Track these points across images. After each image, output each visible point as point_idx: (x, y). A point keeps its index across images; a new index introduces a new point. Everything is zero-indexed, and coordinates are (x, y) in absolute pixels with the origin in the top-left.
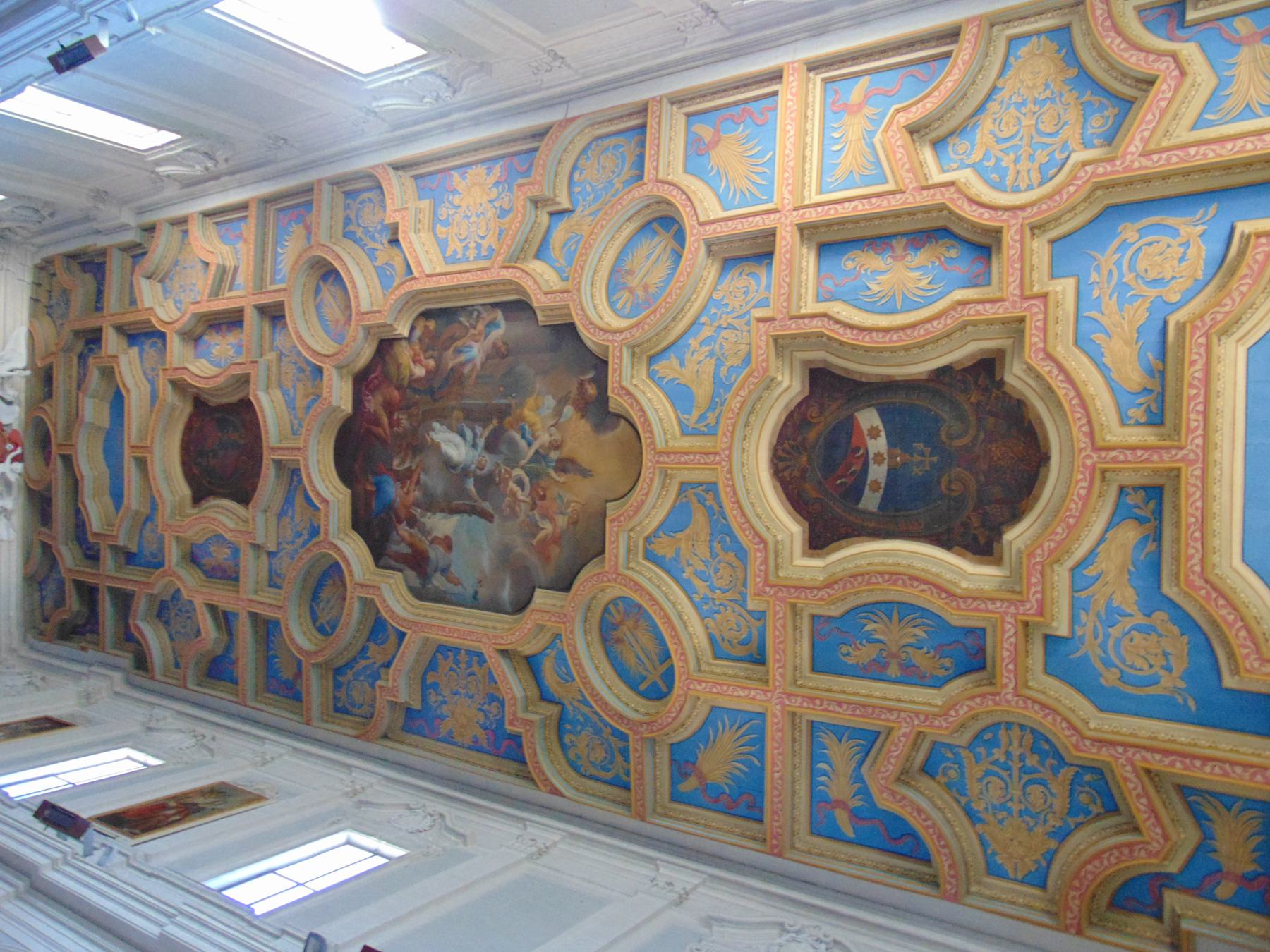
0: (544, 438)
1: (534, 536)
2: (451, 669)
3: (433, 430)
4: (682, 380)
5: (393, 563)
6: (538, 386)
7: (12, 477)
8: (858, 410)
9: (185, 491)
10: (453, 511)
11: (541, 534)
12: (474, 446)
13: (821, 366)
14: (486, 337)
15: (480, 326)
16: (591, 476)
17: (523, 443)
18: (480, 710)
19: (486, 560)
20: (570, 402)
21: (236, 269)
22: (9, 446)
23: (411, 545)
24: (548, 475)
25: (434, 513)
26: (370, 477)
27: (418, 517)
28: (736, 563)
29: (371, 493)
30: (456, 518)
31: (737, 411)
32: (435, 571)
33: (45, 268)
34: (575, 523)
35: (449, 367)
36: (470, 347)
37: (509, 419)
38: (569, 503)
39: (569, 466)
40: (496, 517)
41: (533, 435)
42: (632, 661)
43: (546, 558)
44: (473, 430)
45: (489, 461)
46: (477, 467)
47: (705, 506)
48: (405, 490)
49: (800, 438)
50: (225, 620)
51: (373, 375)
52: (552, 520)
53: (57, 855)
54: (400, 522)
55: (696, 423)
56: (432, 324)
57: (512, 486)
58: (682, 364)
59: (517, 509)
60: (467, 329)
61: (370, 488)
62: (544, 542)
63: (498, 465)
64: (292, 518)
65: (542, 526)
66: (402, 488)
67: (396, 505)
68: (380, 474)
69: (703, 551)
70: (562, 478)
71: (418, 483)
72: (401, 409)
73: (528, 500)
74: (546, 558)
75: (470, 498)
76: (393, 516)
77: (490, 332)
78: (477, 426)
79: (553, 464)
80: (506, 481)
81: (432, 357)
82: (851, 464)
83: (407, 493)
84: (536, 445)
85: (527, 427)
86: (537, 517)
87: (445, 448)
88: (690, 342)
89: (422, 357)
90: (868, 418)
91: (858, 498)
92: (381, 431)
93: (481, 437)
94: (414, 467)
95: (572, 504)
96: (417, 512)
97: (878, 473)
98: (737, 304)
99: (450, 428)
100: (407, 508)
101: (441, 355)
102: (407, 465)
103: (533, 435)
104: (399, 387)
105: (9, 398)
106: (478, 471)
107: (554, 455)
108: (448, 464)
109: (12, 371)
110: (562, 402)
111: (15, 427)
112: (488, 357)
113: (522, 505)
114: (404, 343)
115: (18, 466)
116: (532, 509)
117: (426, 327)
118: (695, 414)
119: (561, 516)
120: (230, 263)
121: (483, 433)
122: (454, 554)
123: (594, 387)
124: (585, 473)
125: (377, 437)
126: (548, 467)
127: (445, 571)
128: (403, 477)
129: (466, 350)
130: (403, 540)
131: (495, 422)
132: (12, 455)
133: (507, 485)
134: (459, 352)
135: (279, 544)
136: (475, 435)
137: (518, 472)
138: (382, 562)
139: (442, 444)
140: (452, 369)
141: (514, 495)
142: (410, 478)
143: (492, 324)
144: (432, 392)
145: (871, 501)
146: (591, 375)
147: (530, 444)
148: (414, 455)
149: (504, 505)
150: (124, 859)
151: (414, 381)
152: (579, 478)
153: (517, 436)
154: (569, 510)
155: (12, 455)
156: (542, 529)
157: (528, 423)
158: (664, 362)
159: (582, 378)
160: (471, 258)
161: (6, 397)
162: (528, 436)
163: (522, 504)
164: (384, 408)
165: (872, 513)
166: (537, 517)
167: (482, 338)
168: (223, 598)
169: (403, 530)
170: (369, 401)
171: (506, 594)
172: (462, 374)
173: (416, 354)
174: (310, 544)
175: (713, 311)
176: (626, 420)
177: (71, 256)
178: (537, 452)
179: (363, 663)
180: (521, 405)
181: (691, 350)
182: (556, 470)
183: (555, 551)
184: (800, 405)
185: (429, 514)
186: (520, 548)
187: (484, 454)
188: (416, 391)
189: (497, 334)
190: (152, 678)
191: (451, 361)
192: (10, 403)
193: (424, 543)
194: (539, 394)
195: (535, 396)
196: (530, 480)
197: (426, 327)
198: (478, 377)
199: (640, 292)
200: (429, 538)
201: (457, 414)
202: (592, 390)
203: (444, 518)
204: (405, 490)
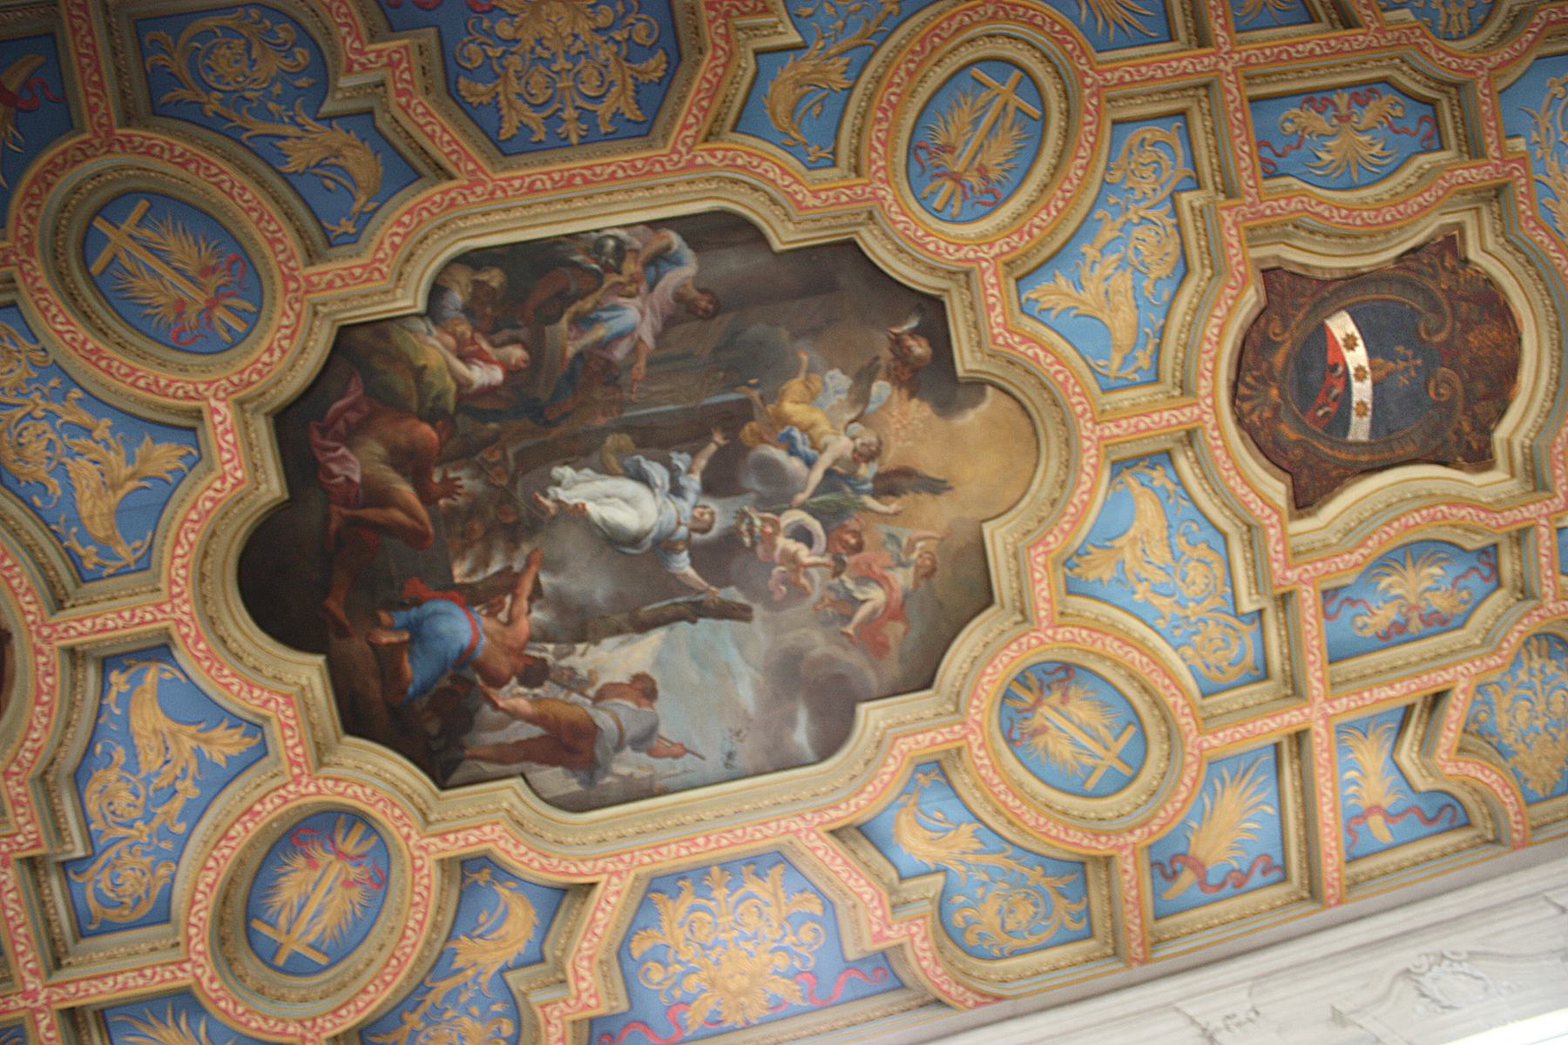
0: (840, 445)
1: (849, 619)
3: (558, 484)
4: (1083, 309)
5: (489, 768)
6: (804, 358)
8: (1329, 316)
10: (643, 627)
13: (1274, 264)
14: (652, 288)
15: (631, 267)
16: (950, 488)
17: (795, 464)
19: (746, 692)
24: (866, 509)
25: (596, 642)
26: (384, 616)
27: (550, 659)
28: (1210, 557)
30: (656, 637)
31: (1214, 339)
32: (619, 747)
34: (930, 574)
35: (571, 351)
38: (911, 546)
39: (903, 482)
40: (758, 610)
42: (1065, 750)
44: (667, 464)
45: (720, 514)
47: (1152, 489)
48: (503, 616)
49: (1264, 366)
51: (340, 404)
52: (881, 581)
54: (498, 682)
55: (1119, 369)
57: (783, 543)
58: (1079, 285)
59: (803, 581)
60: (598, 277)
61: (386, 638)
63: (743, 515)
64: (132, 765)
65: (860, 596)
66: (492, 614)
67: (479, 654)
68: (418, 603)
69: (1160, 554)
70: (893, 506)
71: (537, 592)
72: (445, 460)
73: (826, 559)
75: (691, 590)
77: (658, 278)
78: (674, 455)
79: (869, 486)
80: (769, 540)
81: (514, 341)
82: (1333, 386)
83: (511, 621)
84: (825, 461)
85: (796, 433)
86: (850, 585)
87: (593, 509)
88: (1083, 250)
90: (1341, 326)
91: (1346, 426)
92: (399, 516)
93: (690, 471)
94: (517, 567)
95: (919, 544)
97: (1362, 391)
98: (1147, 188)
99: (605, 470)
100: (517, 652)
102: (495, 567)
104: (433, 415)
106: (697, 537)
107: (867, 471)
108: (613, 540)
110: (863, 378)
112: (669, 322)
113: (813, 571)
114: (422, 326)
116: (836, 574)
118: (1117, 360)
119: (900, 570)
123: (924, 342)
124: (936, 487)
126: (859, 492)
129: (605, 315)
130: (514, 714)
131: (719, 438)
133: (773, 546)
134: (583, 322)
136: (673, 471)
140: (579, 355)
141: (792, 559)
143: (661, 259)
144: (537, 413)
145: (1360, 429)
146: (913, 323)
147: (810, 463)
148: (513, 543)
151: (469, 397)
152: (925, 497)
153: (779, 454)
154: (914, 556)
156: (864, 602)
157: (796, 425)
158: (1046, 286)
159: (896, 330)
160: (574, 139)
163: (814, 571)
164: (397, 467)
165: (1363, 444)
167: (643, 288)
171: (801, 736)
172: (609, 362)
175: (1112, 201)
176: (993, 385)
178: (829, 473)
179: (444, 986)
180: (776, 396)
181: (1089, 261)
182: (876, 494)
183: (894, 630)
184: (1256, 321)
185: (580, 647)
186: (819, 643)
187: (704, 501)
188: (483, 416)
189: (674, 278)
191: (568, 341)
193: (581, 703)
194: (811, 370)
195: (802, 377)
196: (825, 526)
197: (478, 285)
198: (650, 363)
199: (973, 179)
200: (591, 692)
202: (920, 348)
203: (622, 644)
204: (503, 616)
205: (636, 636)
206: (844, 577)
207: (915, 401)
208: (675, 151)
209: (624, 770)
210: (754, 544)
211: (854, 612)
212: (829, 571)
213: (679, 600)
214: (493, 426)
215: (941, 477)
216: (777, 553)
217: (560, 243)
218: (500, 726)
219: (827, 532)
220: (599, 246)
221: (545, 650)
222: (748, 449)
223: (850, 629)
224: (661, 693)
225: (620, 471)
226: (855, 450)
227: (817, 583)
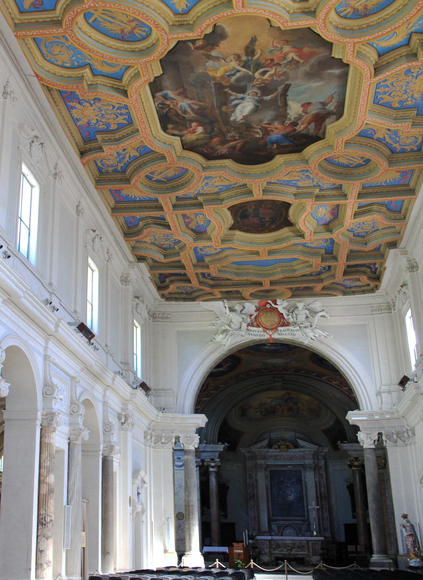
0: (234, 64)
2: (390, 95)
3: (235, 120)
6: (201, 71)
7: (285, 304)
9: (285, 231)
10: (286, 105)
11: (296, 58)
12: (243, 99)
15: (168, 103)
16: (255, 36)
17: (238, 75)
18: (416, 78)
19: (315, 84)
20: (209, 53)
23: (309, 123)
29: (278, 146)
30: (290, 103)
32: (325, 109)
35: (194, 115)
36: (181, 107)
37: (224, 83)
41: (233, 70)
43: (312, 54)
46: (256, 96)
48: (274, 130)
51: (205, 151)
52: (286, 54)
56: (170, 126)
57: (266, 77)
59: (280, 73)
61: (275, 146)
62: (300, 57)
64: (298, 181)
65: (291, 59)
70: (259, 52)
71: (269, 124)
73: (274, 68)
74: (312, 54)
76: (292, 134)
78: (230, 99)
79: (250, 58)
80: (263, 81)
81: (190, 124)
83: (277, 128)
84: (239, 68)
85: (228, 74)
86: (285, 62)
89: (191, 129)
92: (239, 145)
93: (237, 96)
95: (275, 44)
96: (287, 122)
99: (233, 111)
101: (189, 120)
102: (259, 131)
103: (233, 70)
104: (211, 138)
106: (258, 95)
107: (244, 58)
108: (256, 110)
109: (225, 307)
110: (209, 57)
111: (257, 305)
112: (186, 97)
113: (277, 71)
114: (184, 138)
116: (280, 65)
117: (172, 129)
119: (283, 50)
121: (234, 95)
122: (313, 101)
124: (254, 40)
125: (243, 146)
126: (252, 60)
127: (324, 104)
128: (266, 132)
129: (183, 108)
131: (226, 90)
133: (266, 80)
134: (185, 112)
135: (315, 186)
136: (235, 99)
137: (257, 75)
138: (321, 136)
139: (244, 114)
140: (195, 114)
141: (272, 75)
142: (266, 128)
144: (212, 123)
147: (239, 71)
149: (279, 79)
152: (257, 43)
153: (234, 78)
154: (279, 46)
156: (293, 58)
162: (233, 72)
163: (277, 71)
164: (225, 144)
166: (285, 62)
169: (300, 128)
170: (221, 152)
171: (337, 71)
172: (198, 109)
173: (190, 132)
174: (311, 172)
178: (243, 67)
180: (214, 78)
183: (306, 50)
185: (288, 116)
187: (247, 93)
188: (212, 130)
193: (306, 118)
195: (207, 72)
197: (172, 129)
198: (200, 101)
200: (304, 114)
201: (224, 109)
205: (289, 106)
206: (282, 63)
207: (220, 45)
208: (132, 103)
209: (333, 107)
210: (264, 83)
211: (296, 60)
212: (279, 67)
213: (279, 98)
214: (215, 129)
215: (250, 39)
216: (269, 79)
217: (160, 115)
218: (309, 130)
219: (265, 67)
220: (161, 107)
221: (287, 123)
222: (231, 84)
223: (302, 61)
224: (309, 101)
225: (233, 109)
226: (236, 61)
227: (280, 70)
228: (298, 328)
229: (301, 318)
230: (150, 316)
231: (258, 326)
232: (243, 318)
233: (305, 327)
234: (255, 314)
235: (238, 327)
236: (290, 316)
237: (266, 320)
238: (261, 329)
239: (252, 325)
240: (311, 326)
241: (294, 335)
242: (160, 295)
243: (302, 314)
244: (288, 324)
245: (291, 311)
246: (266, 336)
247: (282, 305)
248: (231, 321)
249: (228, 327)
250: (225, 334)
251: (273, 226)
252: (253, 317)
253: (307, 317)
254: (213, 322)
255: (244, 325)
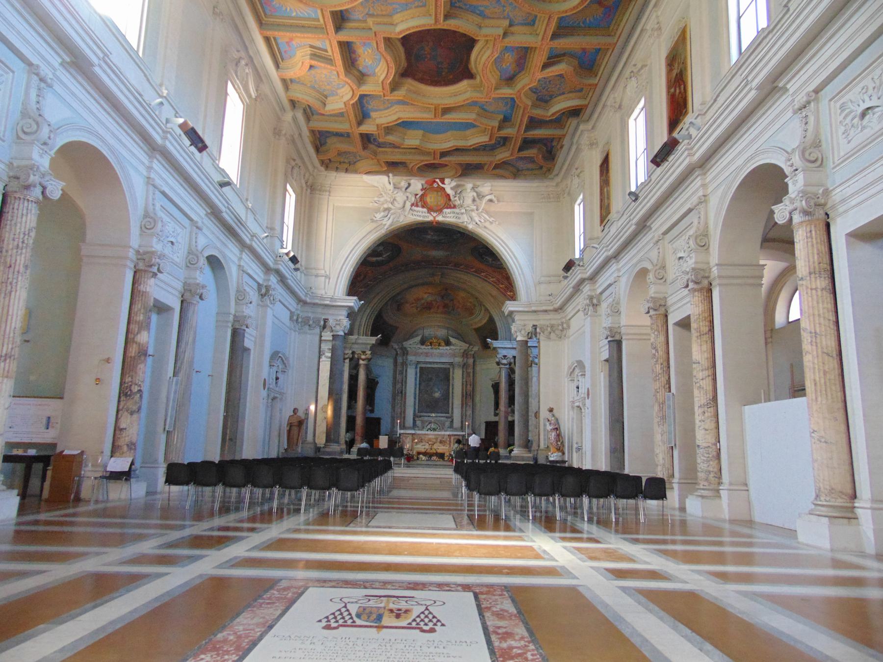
7: (454, 184)
9: (464, 84)
21: (311, 46)
22: (435, 185)
33: (327, 165)
50: (553, 59)
53: (686, 153)
105: (406, 185)
111: (423, 182)
115: (447, 181)
120: (308, 51)
132: (440, 184)
135: (504, 18)
150: (699, 117)
155: (440, 184)
161: (406, 186)
168: (539, 59)
177: (317, 150)
190: (586, 106)
192: (409, 185)
228: (463, 211)
229: (468, 201)
230: (307, 186)
231: (423, 207)
232: (407, 197)
233: (472, 210)
234: (420, 193)
235: (401, 205)
236: (457, 198)
237: (430, 199)
238: (425, 210)
239: (417, 206)
240: (477, 210)
241: (459, 218)
242: (319, 160)
243: (469, 195)
244: (455, 207)
245: (458, 192)
246: (430, 218)
247: (449, 186)
248: (394, 200)
249: (390, 206)
250: (387, 212)
251: (451, 77)
252: (418, 197)
253: (474, 200)
254: (376, 199)
255: (408, 204)
